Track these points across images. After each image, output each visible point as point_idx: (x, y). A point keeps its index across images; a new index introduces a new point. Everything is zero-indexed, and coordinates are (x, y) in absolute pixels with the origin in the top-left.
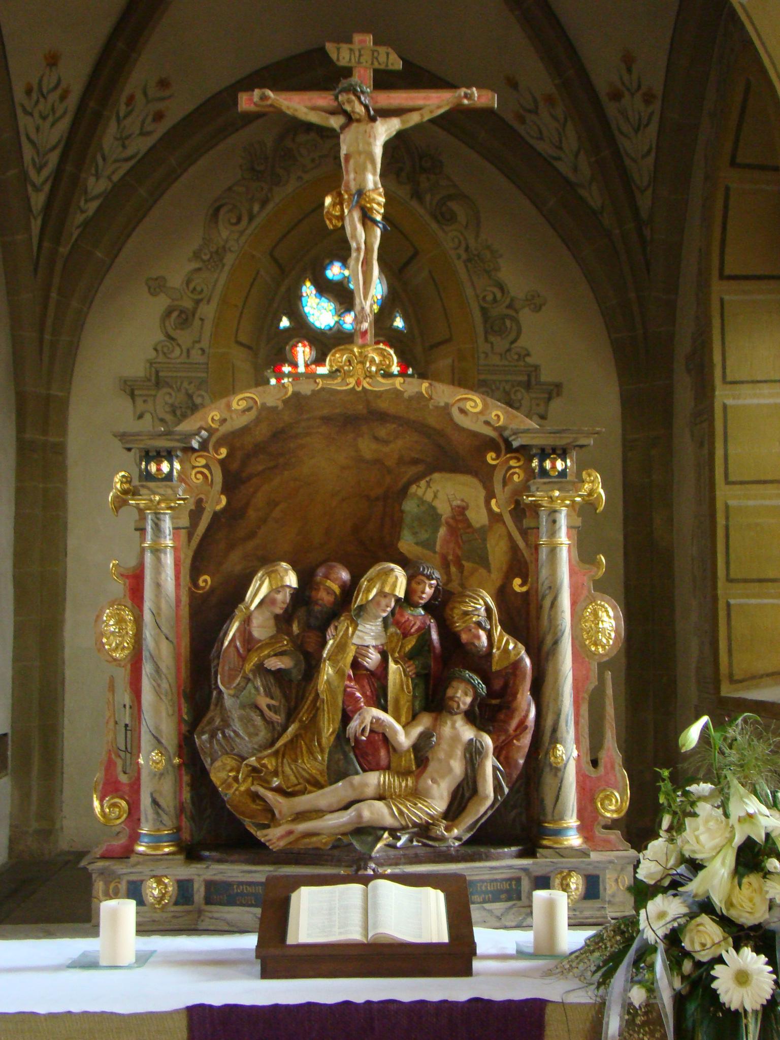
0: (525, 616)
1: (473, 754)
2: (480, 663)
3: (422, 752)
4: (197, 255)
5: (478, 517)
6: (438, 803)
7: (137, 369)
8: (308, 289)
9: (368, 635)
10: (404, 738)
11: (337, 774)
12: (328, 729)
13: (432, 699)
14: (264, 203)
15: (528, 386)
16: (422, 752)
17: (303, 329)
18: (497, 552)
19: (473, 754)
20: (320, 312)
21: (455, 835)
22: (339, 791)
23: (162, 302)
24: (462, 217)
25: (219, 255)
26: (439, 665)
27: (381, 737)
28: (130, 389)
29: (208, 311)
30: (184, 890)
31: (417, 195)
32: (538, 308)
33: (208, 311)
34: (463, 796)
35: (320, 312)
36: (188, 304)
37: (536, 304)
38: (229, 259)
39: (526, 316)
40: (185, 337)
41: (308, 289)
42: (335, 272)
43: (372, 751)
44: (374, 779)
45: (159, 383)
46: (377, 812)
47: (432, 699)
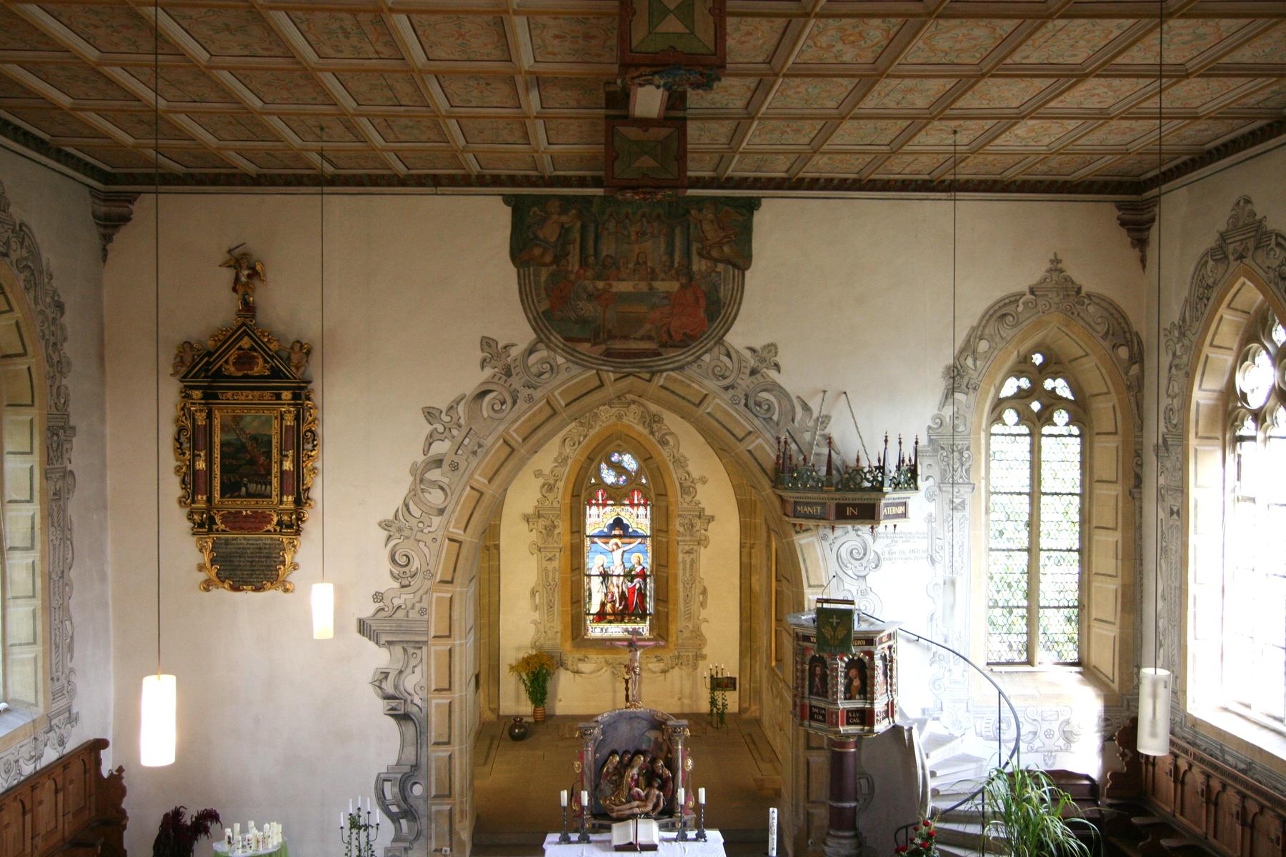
0: (670, 764)
1: (658, 797)
2: (660, 776)
3: (647, 796)
4: (556, 460)
5: (660, 740)
6: (650, 807)
7: (530, 511)
8: (603, 466)
9: (635, 771)
10: (643, 794)
11: (628, 802)
12: (626, 793)
13: (649, 785)
14: (585, 436)
15: (700, 517)
16: (647, 796)
17: (601, 483)
18: (665, 748)
19: (658, 797)
20: (609, 477)
21: (654, 814)
22: (628, 806)
23: (541, 481)
24: (671, 443)
25: (565, 460)
26: (650, 776)
27: (639, 794)
28: (527, 519)
29: (561, 484)
30: (594, 826)
31: (652, 433)
32: (704, 483)
33: (561, 484)
34: (656, 805)
35: (609, 477)
36: (552, 482)
37: (703, 480)
38: (570, 462)
39: (699, 486)
40: (550, 496)
41: (603, 466)
42: (615, 458)
43: (639, 798)
44: (636, 803)
45: (539, 517)
46: (637, 810)
47: (649, 785)
